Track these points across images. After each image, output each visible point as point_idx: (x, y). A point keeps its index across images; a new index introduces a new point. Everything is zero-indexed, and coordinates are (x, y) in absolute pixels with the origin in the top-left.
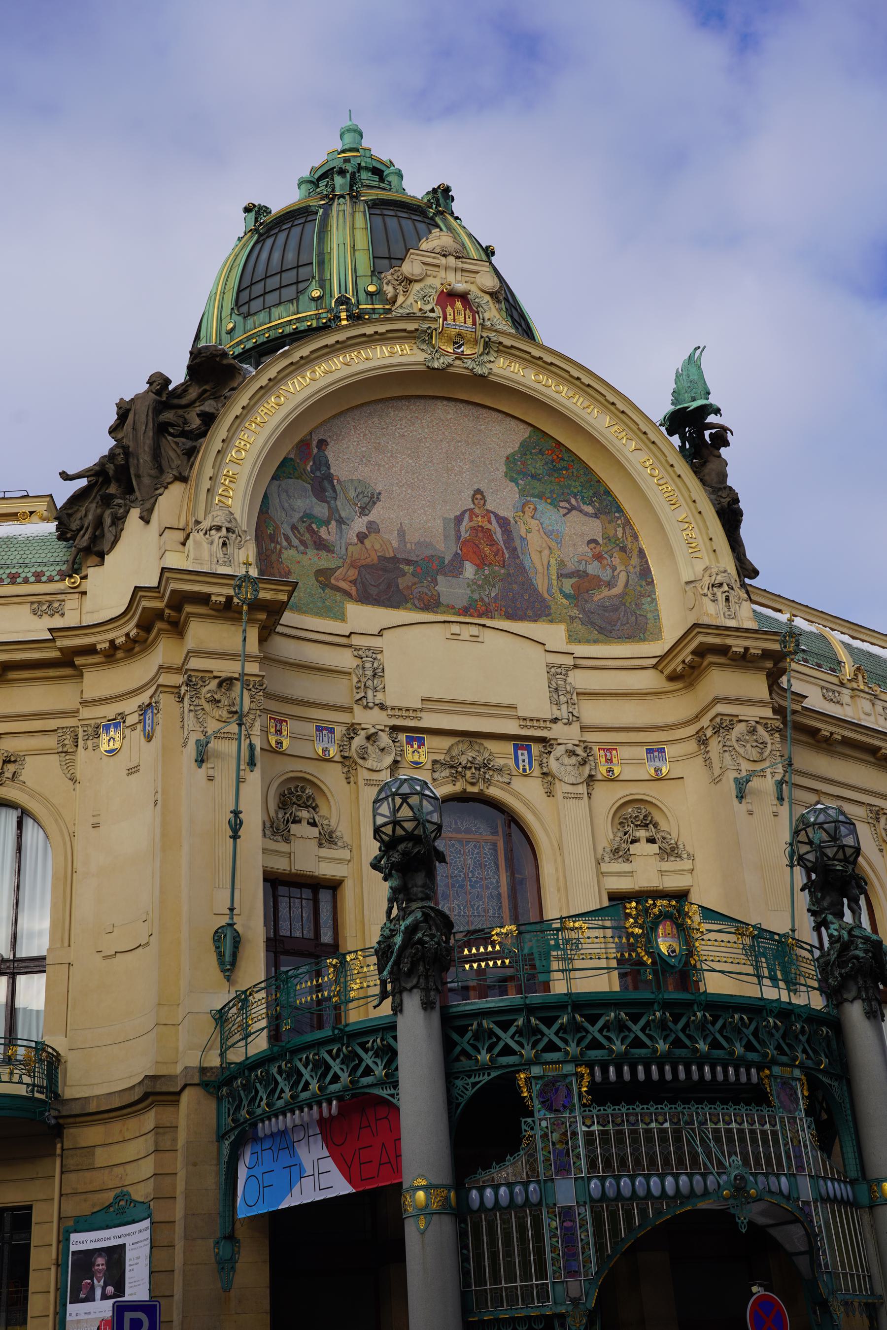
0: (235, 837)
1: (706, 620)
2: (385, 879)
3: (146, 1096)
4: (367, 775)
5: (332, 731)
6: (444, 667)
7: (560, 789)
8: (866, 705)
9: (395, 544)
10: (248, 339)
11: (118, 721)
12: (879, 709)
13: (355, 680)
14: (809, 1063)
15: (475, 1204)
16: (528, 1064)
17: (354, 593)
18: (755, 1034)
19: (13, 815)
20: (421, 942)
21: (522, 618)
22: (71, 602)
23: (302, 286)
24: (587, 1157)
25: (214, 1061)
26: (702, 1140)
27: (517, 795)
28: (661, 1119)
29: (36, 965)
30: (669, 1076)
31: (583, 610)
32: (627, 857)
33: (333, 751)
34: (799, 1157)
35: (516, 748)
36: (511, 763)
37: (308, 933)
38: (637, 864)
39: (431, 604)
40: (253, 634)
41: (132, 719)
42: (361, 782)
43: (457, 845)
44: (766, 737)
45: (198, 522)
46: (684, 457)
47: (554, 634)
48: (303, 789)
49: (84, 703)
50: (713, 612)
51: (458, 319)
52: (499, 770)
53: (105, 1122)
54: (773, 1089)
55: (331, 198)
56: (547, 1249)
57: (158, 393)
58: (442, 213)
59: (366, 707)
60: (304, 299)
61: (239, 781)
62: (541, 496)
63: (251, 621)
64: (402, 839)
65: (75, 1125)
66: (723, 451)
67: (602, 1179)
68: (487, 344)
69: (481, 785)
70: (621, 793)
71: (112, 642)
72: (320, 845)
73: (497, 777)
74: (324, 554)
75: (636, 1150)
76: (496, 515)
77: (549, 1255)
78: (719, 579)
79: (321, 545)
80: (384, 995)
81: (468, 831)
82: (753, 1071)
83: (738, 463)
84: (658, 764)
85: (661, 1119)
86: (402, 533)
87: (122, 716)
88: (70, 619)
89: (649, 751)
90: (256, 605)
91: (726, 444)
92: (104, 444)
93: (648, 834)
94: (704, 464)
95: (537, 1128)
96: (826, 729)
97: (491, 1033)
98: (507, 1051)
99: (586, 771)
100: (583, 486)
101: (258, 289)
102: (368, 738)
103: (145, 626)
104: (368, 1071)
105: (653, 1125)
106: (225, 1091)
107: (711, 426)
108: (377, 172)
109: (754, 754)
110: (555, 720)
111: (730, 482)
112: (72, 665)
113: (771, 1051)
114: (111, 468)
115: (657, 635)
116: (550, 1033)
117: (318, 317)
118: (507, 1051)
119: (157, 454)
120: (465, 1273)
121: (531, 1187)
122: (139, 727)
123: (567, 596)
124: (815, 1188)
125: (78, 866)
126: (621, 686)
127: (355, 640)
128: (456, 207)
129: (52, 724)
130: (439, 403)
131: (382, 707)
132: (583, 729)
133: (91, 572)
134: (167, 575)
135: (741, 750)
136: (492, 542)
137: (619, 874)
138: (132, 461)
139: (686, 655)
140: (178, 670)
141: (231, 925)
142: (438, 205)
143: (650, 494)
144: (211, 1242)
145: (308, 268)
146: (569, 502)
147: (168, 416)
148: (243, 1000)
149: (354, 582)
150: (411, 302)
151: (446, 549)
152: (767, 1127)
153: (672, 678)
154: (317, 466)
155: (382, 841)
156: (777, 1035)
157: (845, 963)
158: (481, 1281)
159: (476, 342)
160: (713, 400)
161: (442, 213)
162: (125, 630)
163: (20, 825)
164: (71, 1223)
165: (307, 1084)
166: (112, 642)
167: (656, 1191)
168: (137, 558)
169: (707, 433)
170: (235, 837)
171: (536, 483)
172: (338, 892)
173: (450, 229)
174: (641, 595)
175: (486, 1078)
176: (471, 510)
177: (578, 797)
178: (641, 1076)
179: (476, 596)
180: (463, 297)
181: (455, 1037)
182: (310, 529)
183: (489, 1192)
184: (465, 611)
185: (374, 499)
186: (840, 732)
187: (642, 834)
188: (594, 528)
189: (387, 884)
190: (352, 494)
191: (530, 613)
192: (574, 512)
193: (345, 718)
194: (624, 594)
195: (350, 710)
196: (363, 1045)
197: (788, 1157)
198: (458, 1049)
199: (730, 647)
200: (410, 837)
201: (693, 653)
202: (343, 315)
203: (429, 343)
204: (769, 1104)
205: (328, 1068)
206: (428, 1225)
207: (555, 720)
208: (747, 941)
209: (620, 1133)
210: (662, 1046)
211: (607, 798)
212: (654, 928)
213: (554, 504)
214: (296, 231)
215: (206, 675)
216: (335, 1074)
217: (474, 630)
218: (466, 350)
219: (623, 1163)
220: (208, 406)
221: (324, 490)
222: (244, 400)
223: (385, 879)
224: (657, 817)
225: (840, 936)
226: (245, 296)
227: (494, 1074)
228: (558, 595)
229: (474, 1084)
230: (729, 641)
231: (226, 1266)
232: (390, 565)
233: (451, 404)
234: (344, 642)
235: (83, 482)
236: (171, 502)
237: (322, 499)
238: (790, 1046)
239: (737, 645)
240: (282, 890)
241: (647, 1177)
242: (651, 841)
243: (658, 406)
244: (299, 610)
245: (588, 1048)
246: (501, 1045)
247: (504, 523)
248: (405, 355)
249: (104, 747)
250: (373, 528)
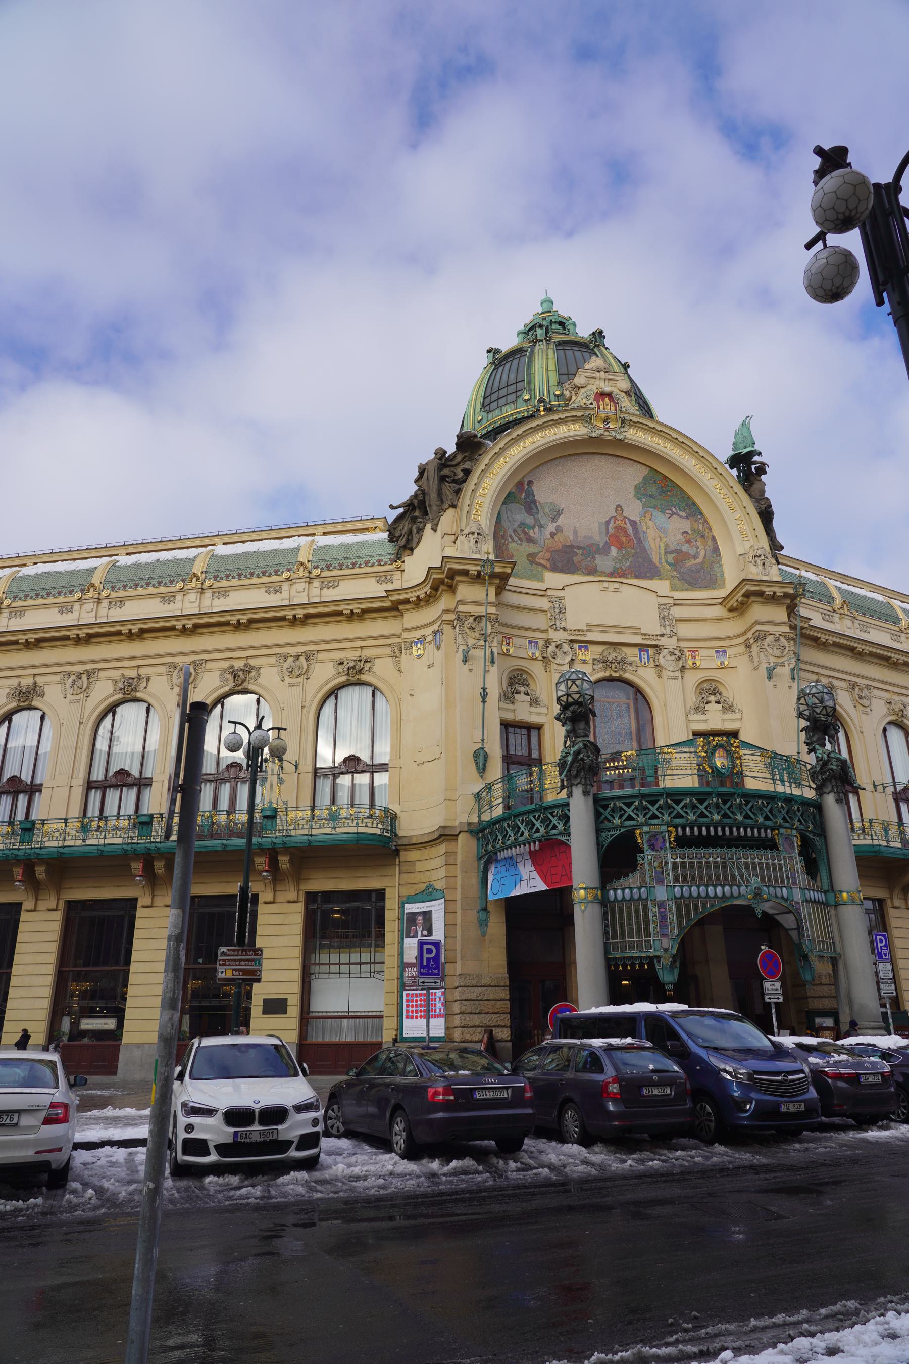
0: (484, 702)
1: (751, 577)
2: (563, 726)
3: (441, 836)
4: (556, 667)
5: (537, 643)
6: (599, 606)
7: (665, 673)
8: (848, 622)
9: (571, 538)
10: (490, 425)
11: (422, 640)
12: (857, 625)
13: (549, 615)
14: (802, 827)
15: (612, 898)
16: (642, 825)
17: (548, 566)
18: (771, 811)
19: (370, 690)
20: (582, 760)
21: (644, 578)
22: (397, 576)
23: (519, 393)
24: (674, 875)
25: (476, 820)
26: (738, 868)
27: (641, 678)
28: (715, 856)
29: (383, 768)
30: (720, 833)
31: (679, 572)
32: (704, 712)
33: (538, 654)
34: (794, 878)
35: (640, 651)
36: (638, 659)
37: (525, 753)
38: (709, 715)
39: (592, 571)
40: (492, 591)
41: (429, 639)
42: (553, 671)
43: (607, 705)
44: (785, 643)
45: (462, 530)
46: (739, 482)
47: (662, 586)
48: (521, 675)
49: (404, 630)
50: (755, 572)
51: (607, 408)
52: (630, 664)
53: (420, 848)
54: (780, 841)
55: (535, 342)
56: (651, 922)
57: (440, 459)
58: (598, 346)
59: (556, 630)
60: (520, 401)
61: (486, 671)
62: (655, 508)
63: (490, 584)
64: (571, 704)
65: (405, 850)
66: (763, 477)
67: (682, 887)
68: (623, 422)
69: (620, 672)
70: (699, 676)
71: (418, 597)
72: (531, 705)
73: (629, 667)
74: (532, 545)
75: (701, 872)
76: (629, 519)
77: (651, 926)
78: (759, 552)
79: (530, 540)
80: (563, 787)
81: (613, 698)
82: (769, 831)
83: (771, 484)
84: (722, 659)
85: (715, 856)
86: (575, 532)
87: (424, 637)
88: (396, 585)
89: (717, 652)
90: (493, 575)
91: (765, 473)
92: (410, 489)
93: (716, 699)
94: (751, 485)
95: (646, 859)
96: (823, 637)
97: (621, 809)
98: (630, 818)
99: (680, 663)
100: (679, 501)
101: (495, 397)
102: (557, 647)
103: (435, 588)
104: (555, 827)
105: (711, 859)
106: (480, 835)
107: (755, 463)
108: (562, 324)
109: (778, 653)
110: (663, 635)
111: (766, 495)
112: (397, 609)
113: (779, 821)
114: (416, 502)
115: (723, 586)
116: (654, 809)
117: (528, 410)
118: (630, 818)
119: (440, 493)
120: (607, 933)
121: (643, 890)
122: (433, 642)
123: (670, 565)
124: (803, 894)
125: (403, 716)
126: (702, 616)
127: (549, 593)
128: (606, 342)
129: (389, 641)
130: (596, 456)
131: (565, 629)
132: (679, 640)
133: (406, 559)
134: (445, 560)
135: (770, 651)
136: (627, 535)
137: (699, 721)
138: (427, 498)
139: (739, 597)
140: (453, 612)
141: (482, 749)
142: (596, 341)
143: (718, 504)
144: (475, 912)
145: (521, 383)
146: (671, 510)
147: (446, 471)
148: (489, 788)
149: (548, 560)
150: (579, 400)
151: (600, 539)
152: (776, 861)
153: (731, 610)
154: (527, 496)
155: (561, 705)
156: (784, 812)
157: (826, 772)
158: (615, 937)
159: (617, 420)
160: (757, 447)
161: (598, 346)
162: (424, 591)
163: (373, 695)
164: (405, 899)
165: (523, 833)
166: (418, 597)
167: (711, 894)
168: (431, 550)
169: (753, 467)
170: (484, 702)
171: (652, 500)
172: (542, 731)
173: (603, 356)
174: (713, 563)
175: (618, 832)
176: (615, 517)
177: (675, 678)
178: (704, 833)
179: (618, 566)
180: (609, 395)
181: (601, 810)
182: (524, 531)
183: (619, 892)
184: (611, 575)
185: (559, 513)
186: (831, 639)
187: (712, 698)
188: (686, 525)
189: (564, 728)
190: (547, 511)
191: (648, 574)
192: (674, 516)
193: (544, 636)
194: (703, 563)
195: (547, 631)
196: (552, 814)
197: (788, 878)
198: (603, 817)
199: (764, 592)
200: (576, 703)
201: (743, 596)
202: (542, 409)
203: (590, 422)
204: (777, 849)
205: (534, 825)
206: (586, 908)
207: (663, 635)
208: (767, 760)
209: (693, 863)
210: (716, 817)
211: (692, 678)
212: (713, 753)
213: (663, 512)
214: (515, 362)
215: (468, 614)
216: (538, 829)
217: (616, 585)
218: (611, 425)
219: (693, 879)
220: (467, 465)
221: (531, 509)
222: (486, 461)
223: (563, 726)
224: (721, 689)
225: (822, 758)
226: (487, 401)
227: (622, 830)
228: (665, 564)
229: (611, 836)
230: (764, 589)
231: (483, 924)
233: (603, 457)
234: (543, 594)
235: (402, 510)
236: (448, 519)
237: (530, 514)
238: (790, 818)
239: (769, 591)
240: (511, 730)
241: (707, 887)
242: (718, 702)
243: (725, 453)
244: (518, 576)
245: (675, 817)
246: (626, 815)
247: (634, 524)
248: (576, 430)
249: (415, 654)
250: (559, 529)
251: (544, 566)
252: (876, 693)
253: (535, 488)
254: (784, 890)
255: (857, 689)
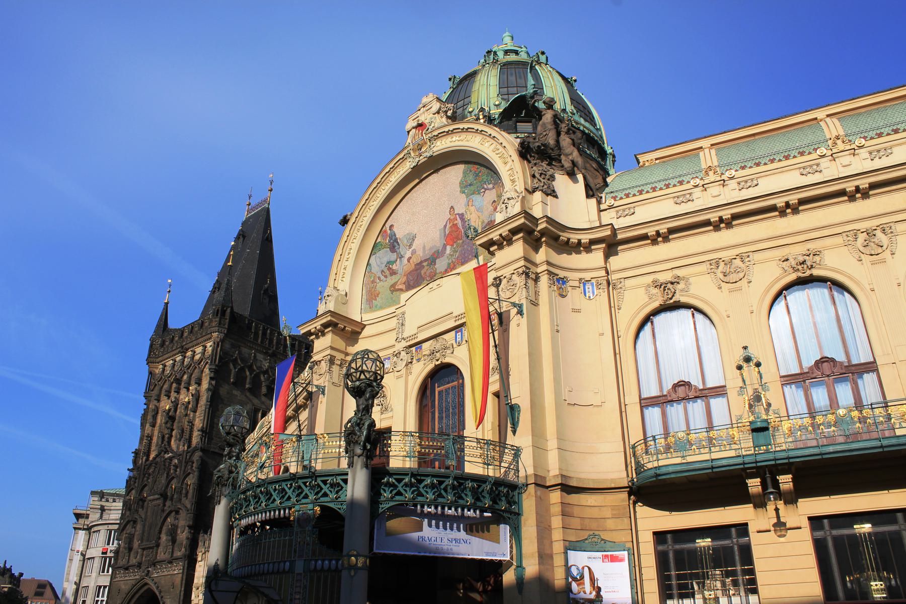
39: (433, 278)
73: (449, 352)
79: (393, 273)
86: (424, 247)
154: (391, 238)
182: (389, 269)
184: (446, 271)
197: (295, 551)
213: (479, 193)
221: (394, 247)
230: (490, 237)
232: (419, 265)
247: (462, 216)
250: (414, 252)
251: (401, 290)
252: (757, 257)
253: (395, 229)
254: (288, 564)
255: (722, 265)
